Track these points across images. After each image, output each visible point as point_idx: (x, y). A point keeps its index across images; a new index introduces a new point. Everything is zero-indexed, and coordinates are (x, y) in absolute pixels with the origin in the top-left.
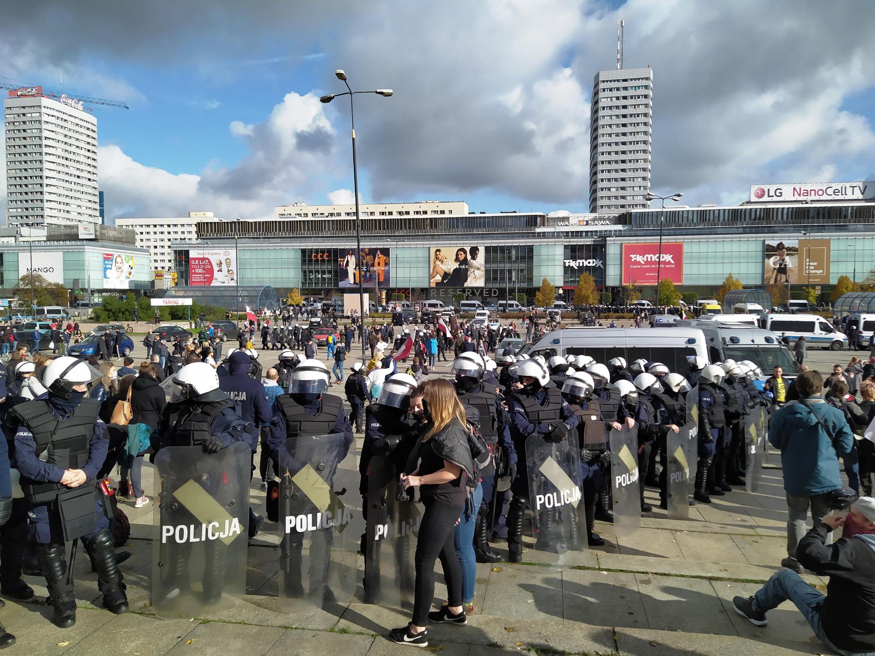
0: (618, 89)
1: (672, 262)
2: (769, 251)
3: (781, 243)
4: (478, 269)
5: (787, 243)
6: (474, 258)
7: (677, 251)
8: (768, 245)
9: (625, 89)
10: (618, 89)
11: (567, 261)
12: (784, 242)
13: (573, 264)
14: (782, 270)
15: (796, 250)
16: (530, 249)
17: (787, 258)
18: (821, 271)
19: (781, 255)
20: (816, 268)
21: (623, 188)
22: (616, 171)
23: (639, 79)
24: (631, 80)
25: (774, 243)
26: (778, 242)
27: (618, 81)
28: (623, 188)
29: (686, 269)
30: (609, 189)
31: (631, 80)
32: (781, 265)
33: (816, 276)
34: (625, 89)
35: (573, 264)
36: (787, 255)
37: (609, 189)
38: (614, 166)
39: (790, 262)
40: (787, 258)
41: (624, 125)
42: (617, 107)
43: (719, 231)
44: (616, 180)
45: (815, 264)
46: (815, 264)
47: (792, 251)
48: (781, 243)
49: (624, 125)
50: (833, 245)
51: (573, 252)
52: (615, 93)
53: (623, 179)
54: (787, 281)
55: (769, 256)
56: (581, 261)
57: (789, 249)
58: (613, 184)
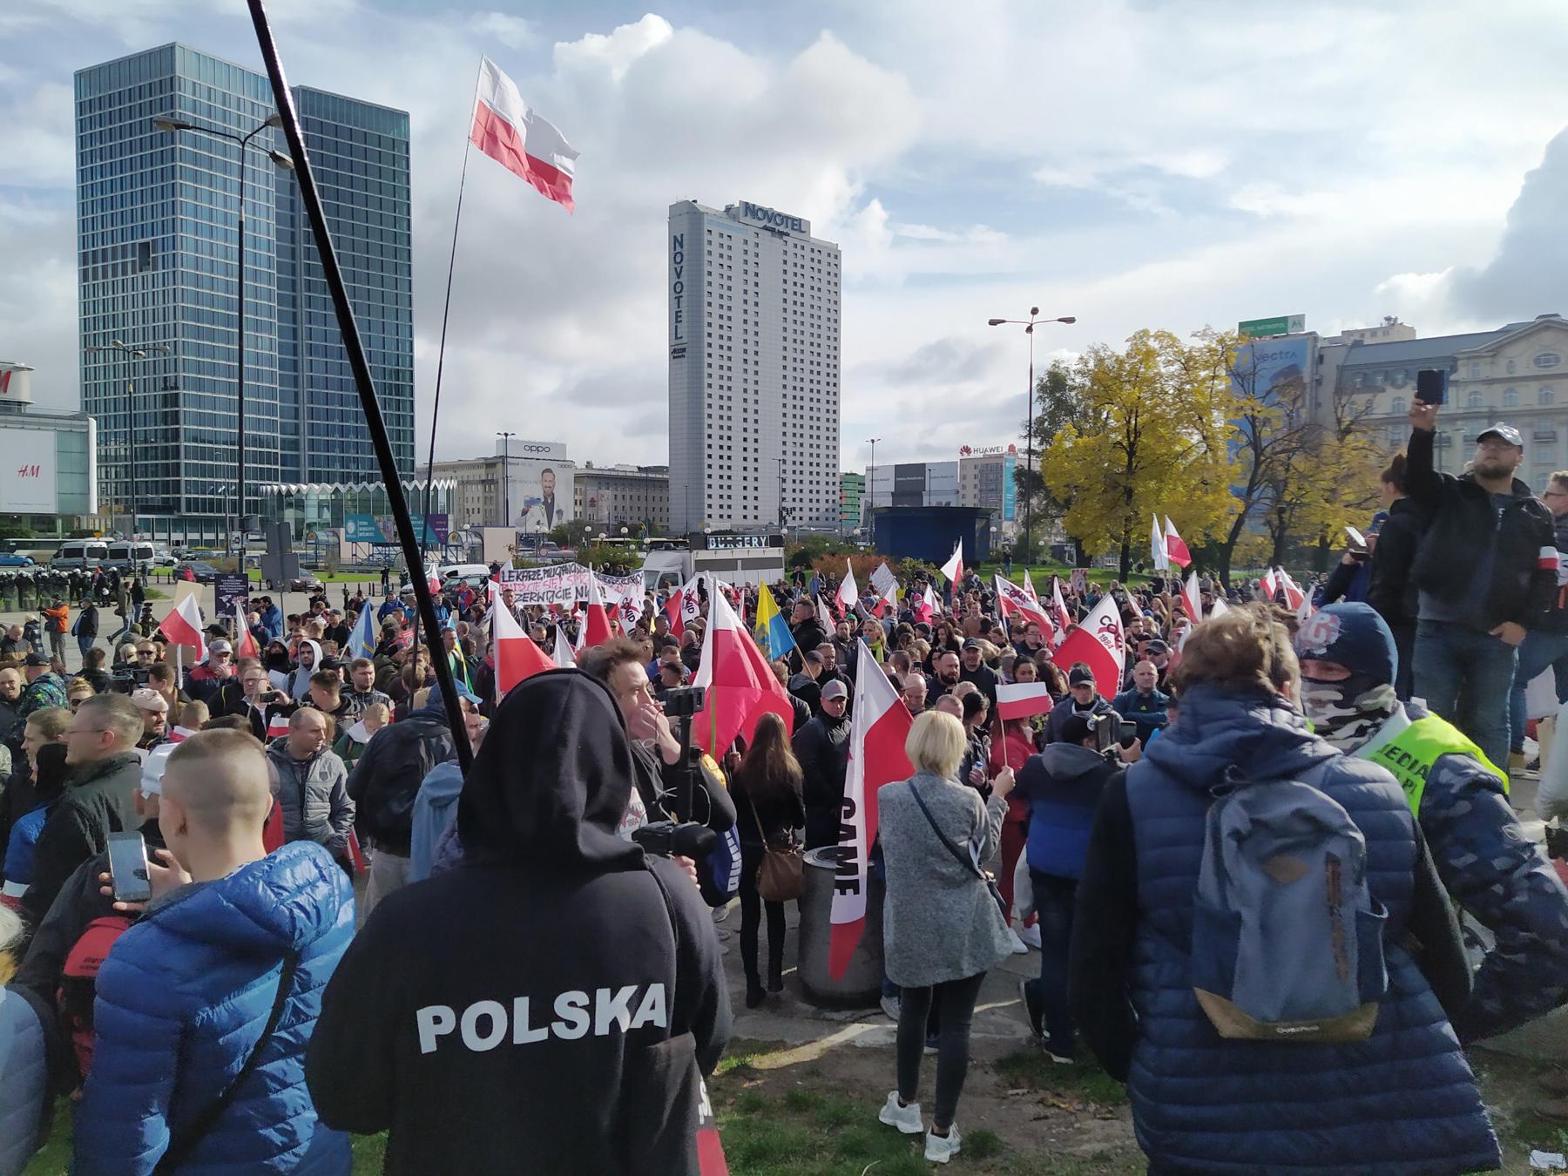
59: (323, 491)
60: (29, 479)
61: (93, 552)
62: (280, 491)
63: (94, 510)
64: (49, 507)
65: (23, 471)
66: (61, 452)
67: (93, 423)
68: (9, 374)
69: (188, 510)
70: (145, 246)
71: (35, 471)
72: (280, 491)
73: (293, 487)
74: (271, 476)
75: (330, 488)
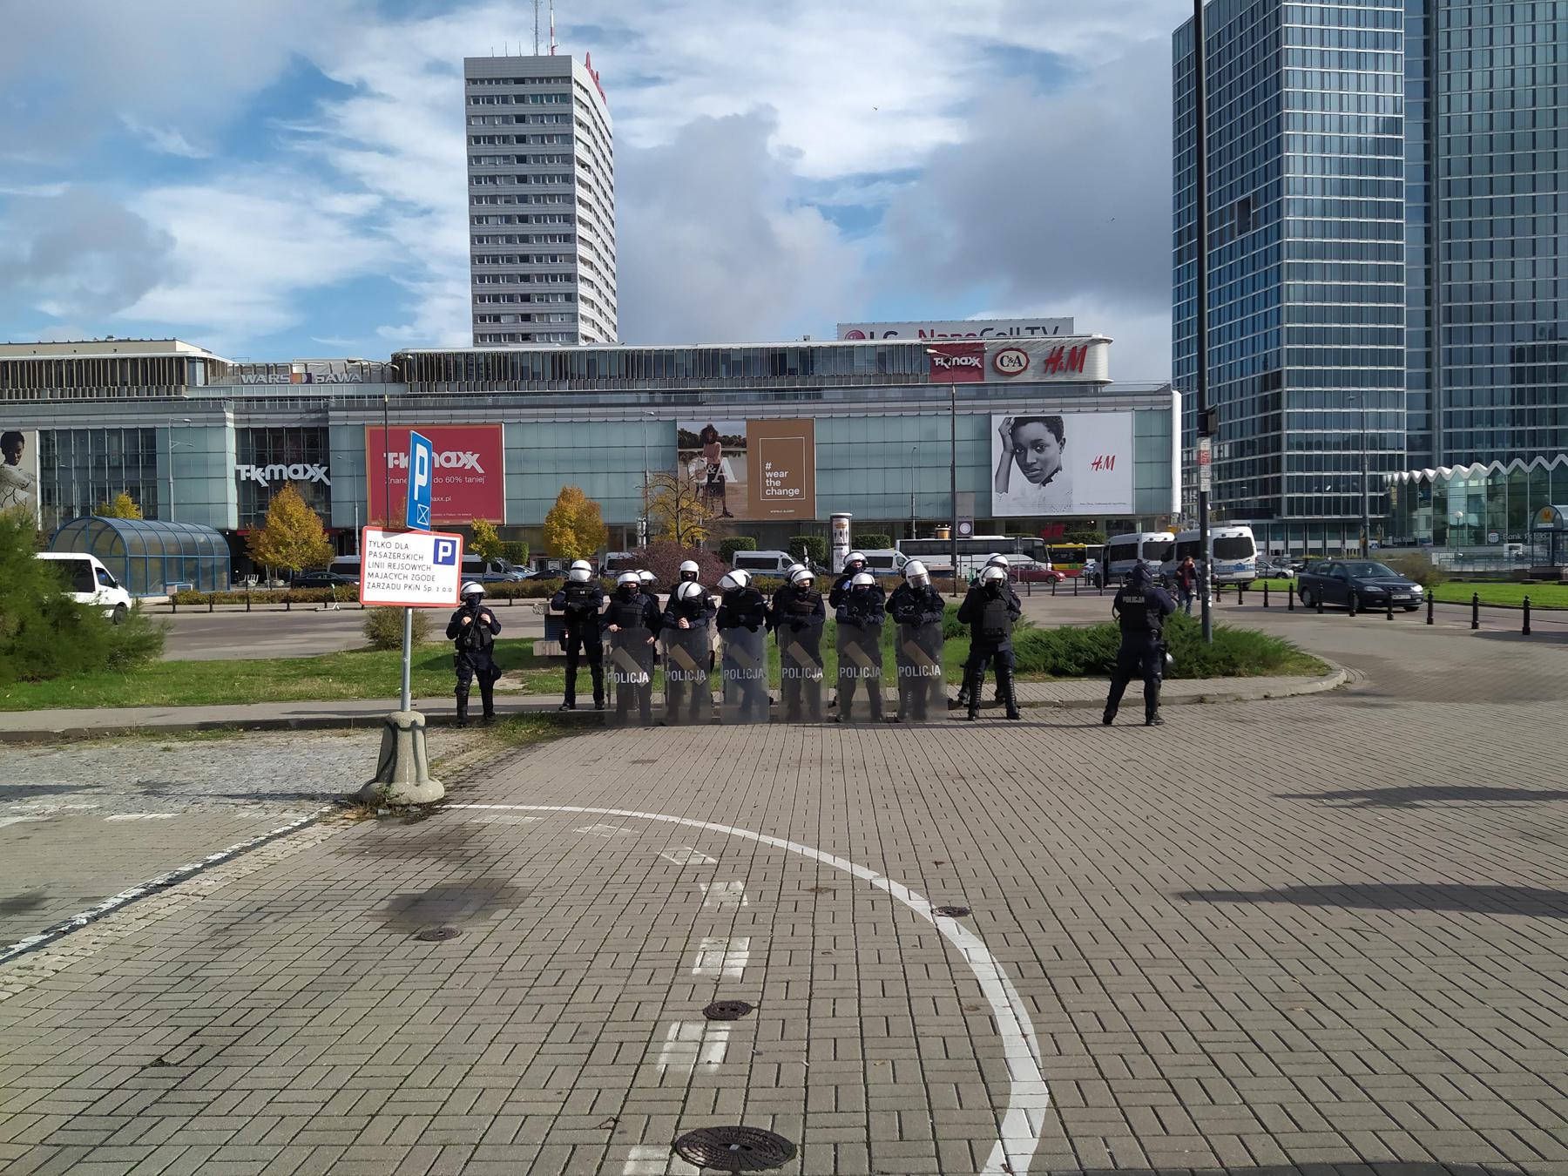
0: (505, 99)
1: (480, 471)
2: (688, 445)
3: (710, 429)
4: (24, 487)
5: (723, 428)
6: (11, 460)
7: (485, 442)
8: (683, 432)
9: (520, 99)
10: (505, 99)
11: (243, 468)
12: (716, 426)
13: (256, 474)
14: (716, 487)
15: (743, 444)
16: (150, 435)
17: (725, 463)
18: (797, 491)
19: (712, 456)
20: (785, 484)
21: (526, 318)
22: (510, 278)
23: (548, 80)
24: (533, 80)
25: (696, 428)
26: (704, 425)
27: (506, 81)
28: (526, 318)
29: (508, 488)
30: (497, 318)
31: (533, 80)
32: (711, 477)
33: (784, 502)
34: (520, 99)
35: (256, 474)
36: (725, 454)
37: (497, 318)
38: (505, 268)
39: (730, 470)
40: (725, 463)
41: (523, 179)
42: (506, 139)
43: (602, 399)
44: (511, 298)
45: (783, 474)
46: (783, 474)
47: (734, 445)
48: (710, 429)
49: (523, 179)
50: (821, 433)
51: (260, 445)
52: (499, 108)
53: (526, 298)
54: (726, 514)
55: (686, 459)
56: (276, 468)
57: (727, 441)
58: (503, 307)
59: (1474, 476)
60: (1104, 472)
61: (1152, 549)
62: (1411, 479)
63: (1177, 508)
64: (1127, 509)
65: (1097, 464)
66: (1140, 437)
67: (1177, 397)
68: (1085, 348)
69: (1291, 513)
70: (1245, 204)
71: (1110, 463)
72: (1411, 479)
73: (1431, 473)
74: (1394, 463)
75: (1483, 469)
